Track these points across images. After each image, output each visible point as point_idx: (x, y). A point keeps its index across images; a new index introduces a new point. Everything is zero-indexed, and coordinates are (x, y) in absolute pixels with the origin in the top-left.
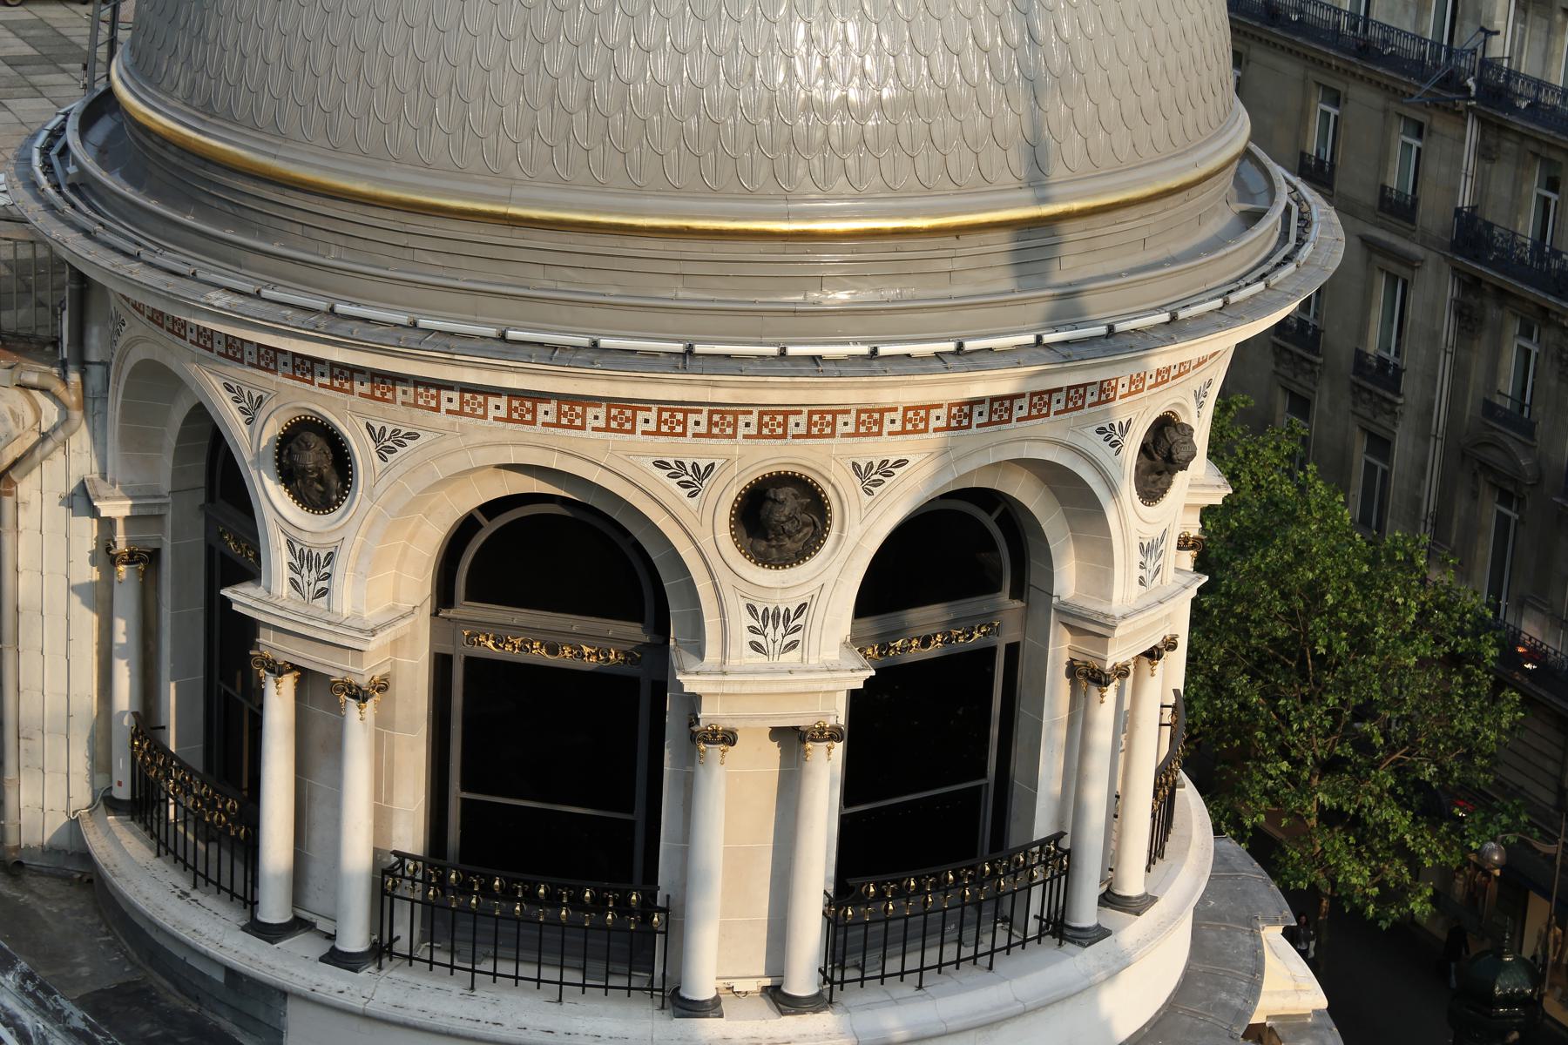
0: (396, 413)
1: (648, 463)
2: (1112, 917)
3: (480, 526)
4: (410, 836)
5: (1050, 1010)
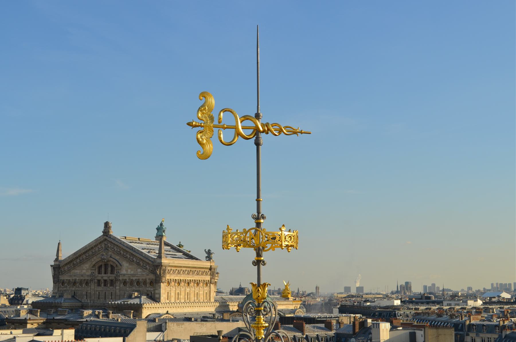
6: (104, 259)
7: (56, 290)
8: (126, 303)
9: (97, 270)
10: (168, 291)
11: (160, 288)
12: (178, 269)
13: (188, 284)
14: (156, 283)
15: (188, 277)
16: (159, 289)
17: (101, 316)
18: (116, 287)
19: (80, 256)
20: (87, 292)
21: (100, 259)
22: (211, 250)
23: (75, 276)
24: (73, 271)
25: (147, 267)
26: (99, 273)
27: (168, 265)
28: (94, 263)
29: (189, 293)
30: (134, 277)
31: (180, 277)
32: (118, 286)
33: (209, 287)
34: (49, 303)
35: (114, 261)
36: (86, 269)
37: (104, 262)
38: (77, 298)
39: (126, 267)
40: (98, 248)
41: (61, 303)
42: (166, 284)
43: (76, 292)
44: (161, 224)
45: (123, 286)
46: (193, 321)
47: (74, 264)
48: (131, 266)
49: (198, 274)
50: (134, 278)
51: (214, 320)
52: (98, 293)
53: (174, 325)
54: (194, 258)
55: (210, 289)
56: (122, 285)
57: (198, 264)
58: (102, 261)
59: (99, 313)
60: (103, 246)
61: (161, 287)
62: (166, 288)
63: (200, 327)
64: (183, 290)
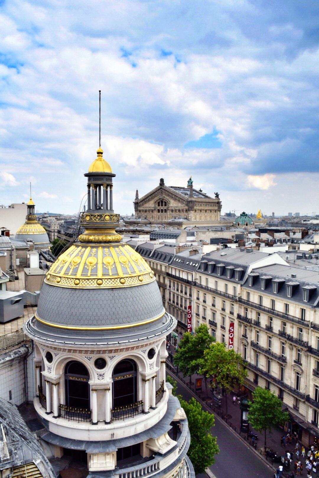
0: (56, 352)
1: (84, 357)
2: (151, 410)
3: (69, 364)
4: (63, 402)
5: (141, 423)
14: (189, 211)
19: (148, 197)
23: (146, 207)
26: (159, 205)
28: (155, 201)
32: (169, 212)
35: (166, 199)
44: (190, 179)
47: (145, 201)
48: (175, 202)
49: (211, 206)
50: (177, 208)
56: (171, 212)
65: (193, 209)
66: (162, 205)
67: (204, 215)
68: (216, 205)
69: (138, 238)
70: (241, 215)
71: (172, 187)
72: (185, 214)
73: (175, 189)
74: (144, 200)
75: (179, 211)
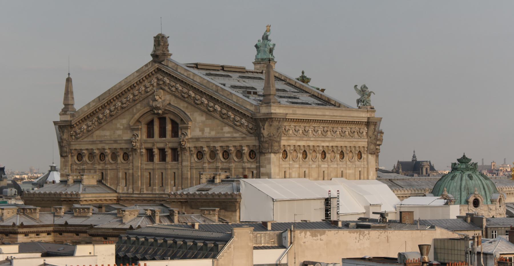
6: (158, 108)
7: (65, 169)
8: (203, 193)
9: (144, 130)
10: (285, 168)
11: (269, 163)
12: (302, 125)
13: (324, 154)
14: (262, 153)
15: (324, 141)
16: (268, 166)
17: (157, 218)
18: (182, 162)
19: (109, 103)
20: (126, 173)
21: (147, 109)
22: (367, 86)
23: (101, 142)
24: (97, 133)
25: (243, 121)
26: (150, 134)
27: (283, 119)
28: (137, 116)
29: (326, 172)
30: (217, 141)
31: (308, 142)
33: (365, 160)
34: (55, 194)
35: (176, 111)
36: (122, 127)
37: (158, 114)
38: (109, 185)
39: (201, 124)
40: (146, 88)
41: (77, 194)
42: (281, 155)
43: (104, 173)
44: (265, 38)
45: (196, 160)
46: (339, 228)
47: (99, 118)
48: (209, 122)
49: (343, 134)
50: (218, 145)
51: (383, 225)
52: (146, 174)
53: (306, 234)
54: (333, 103)
55: (368, 164)
57: (343, 115)
58: (152, 112)
59: (153, 212)
60: (154, 81)
61: (272, 160)
62: (282, 162)
63: (358, 239)
64: (314, 166)
65: (276, 148)
66: (163, 134)
67: (319, 166)
68: (360, 133)
69: (71, 254)
70: (454, 168)
71: (196, 66)
72: (248, 165)
73: (207, 75)
74: (93, 114)
75: (226, 154)
